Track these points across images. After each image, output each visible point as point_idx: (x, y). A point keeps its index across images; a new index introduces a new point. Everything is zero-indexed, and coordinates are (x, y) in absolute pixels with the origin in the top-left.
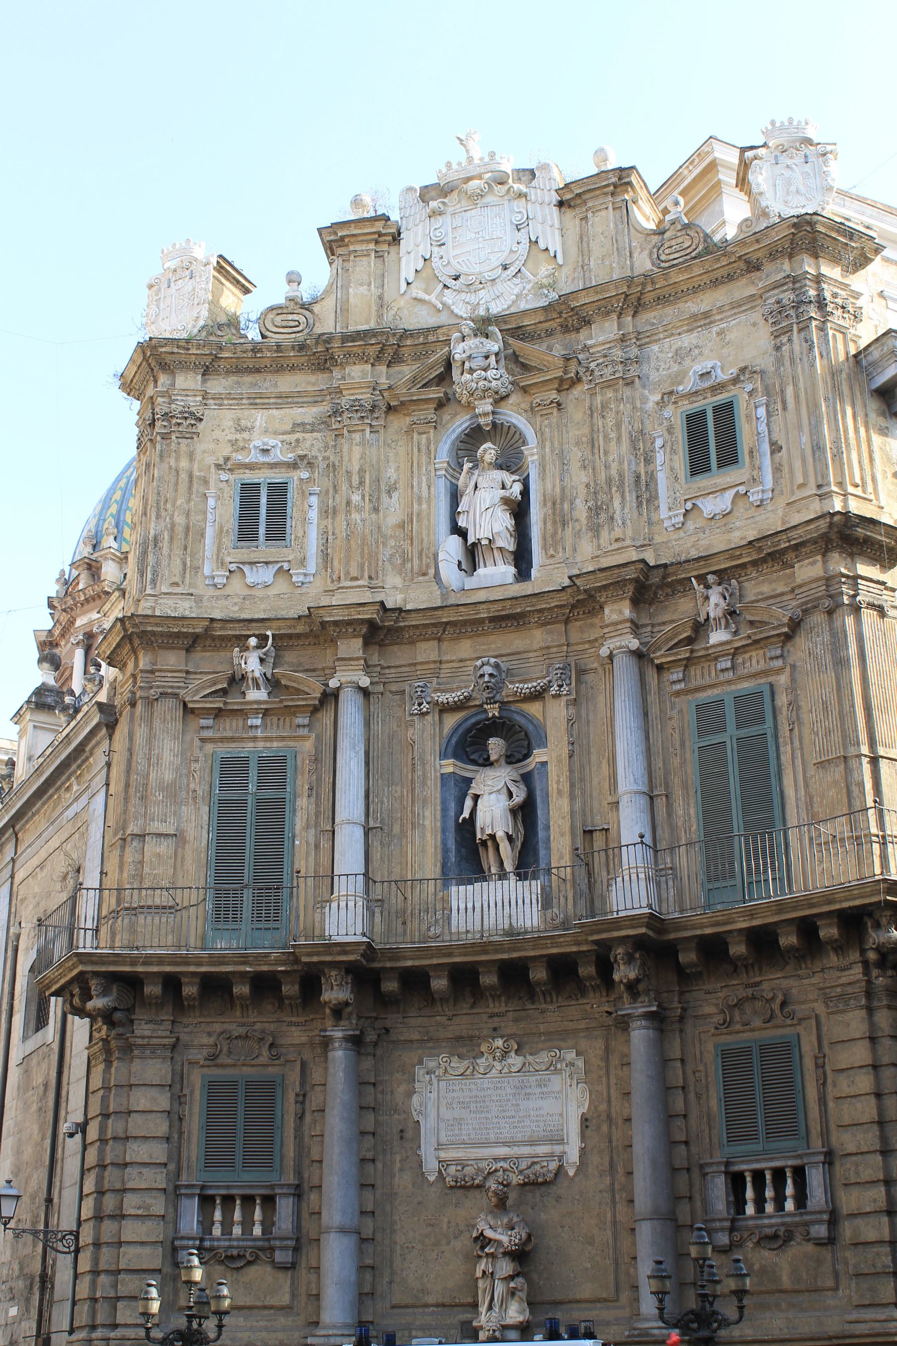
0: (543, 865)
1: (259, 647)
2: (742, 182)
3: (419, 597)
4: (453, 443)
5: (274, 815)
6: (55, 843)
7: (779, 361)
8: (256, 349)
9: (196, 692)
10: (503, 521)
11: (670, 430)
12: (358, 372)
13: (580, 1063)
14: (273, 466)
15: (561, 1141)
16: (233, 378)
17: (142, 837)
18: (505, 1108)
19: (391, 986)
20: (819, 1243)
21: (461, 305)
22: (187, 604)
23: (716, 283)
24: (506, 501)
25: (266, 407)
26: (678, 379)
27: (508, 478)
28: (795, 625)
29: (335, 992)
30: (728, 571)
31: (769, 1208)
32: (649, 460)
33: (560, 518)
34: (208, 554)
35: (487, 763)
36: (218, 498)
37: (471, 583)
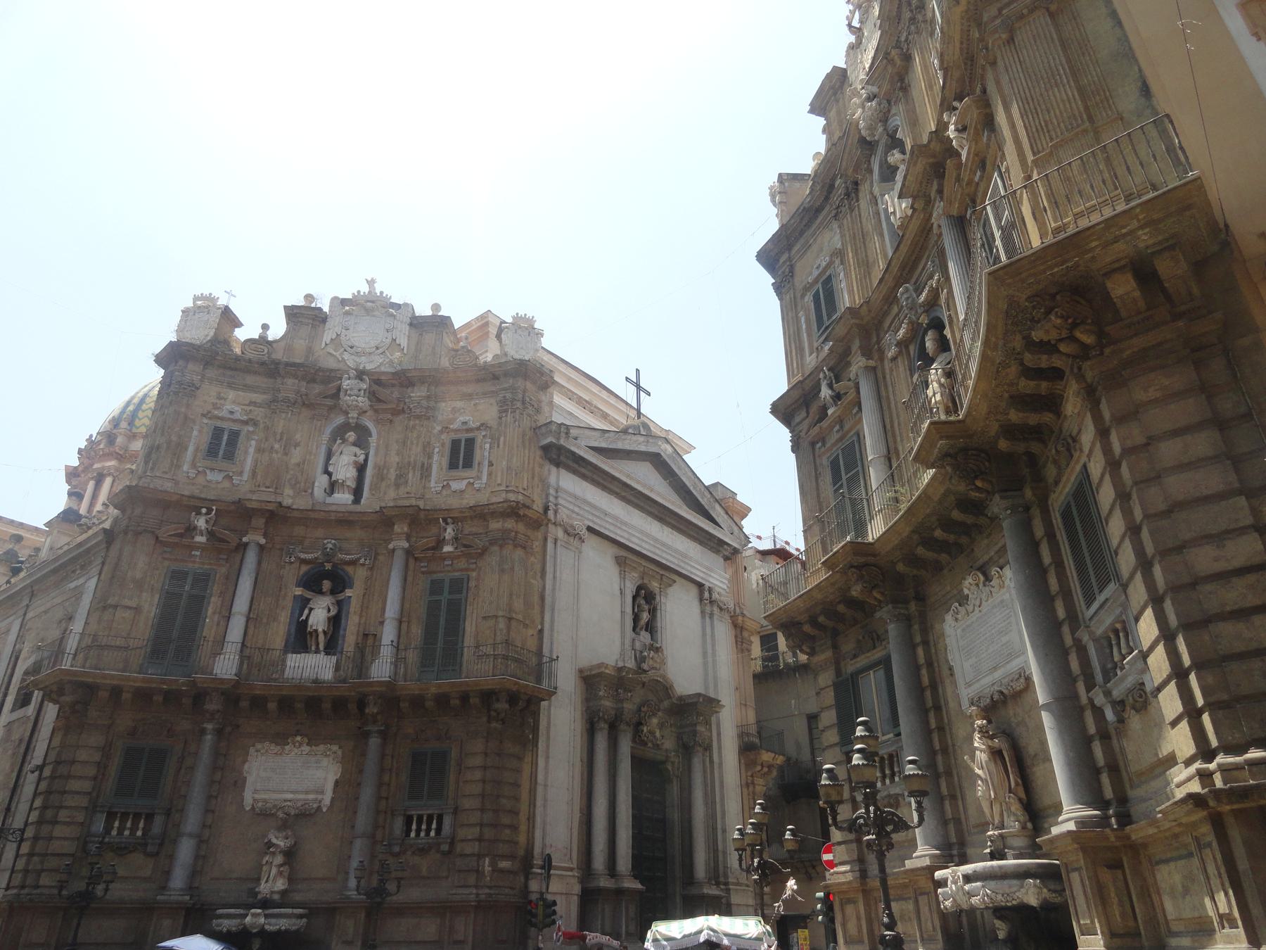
0: (339, 649)
1: (208, 513)
2: (498, 337)
3: (302, 503)
4: (332, 432)
5: (197, 604)
6: (58, 600)
7: (500, 424)
8: (237, 359)
11: (443, 445)
13: (340, 753)
15: (322, 792)
17: (115, 607)
18: (294, 775)
20: (444, 854)
21: (351, 361)
22: (170, 485)
23: (478, 381)
24: (356, 463)
25: (235, 389)
26: (452, 421)
28: (484, 551)
29: (212, 705)
30: (456, 518)
31: (422, 834)
32: (430, 457)
33: (380, 476)
35: (320, 592)
36: (200, 431)
37: (329, 500)
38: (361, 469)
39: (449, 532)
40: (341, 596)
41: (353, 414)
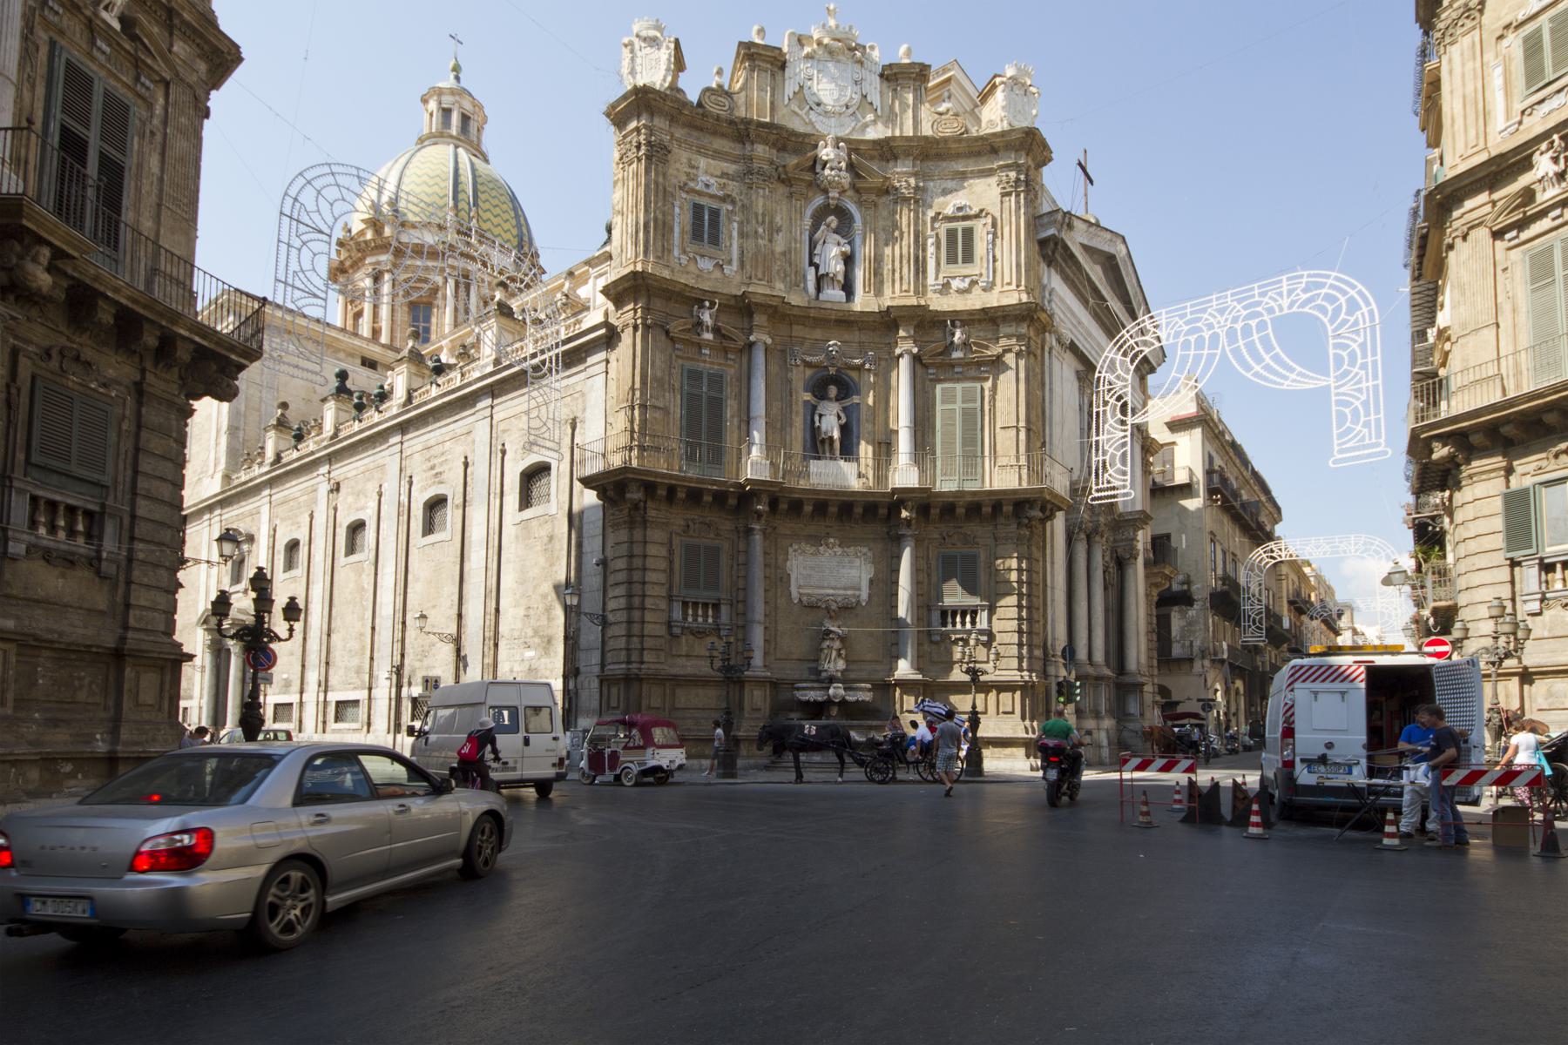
3: (795, 299)
5: (717, 405)
9: (676, 327)
10: (840, 267)
12: (761, 150)
14: (712, 196)
16: (686, 130)
19: (784, 506)
25: (706, 156)
27: (843, 241)
34: (677, 242)
38: (849, 260)
39: (958, 336)
40: (847, 402)
41: (833, 194)
